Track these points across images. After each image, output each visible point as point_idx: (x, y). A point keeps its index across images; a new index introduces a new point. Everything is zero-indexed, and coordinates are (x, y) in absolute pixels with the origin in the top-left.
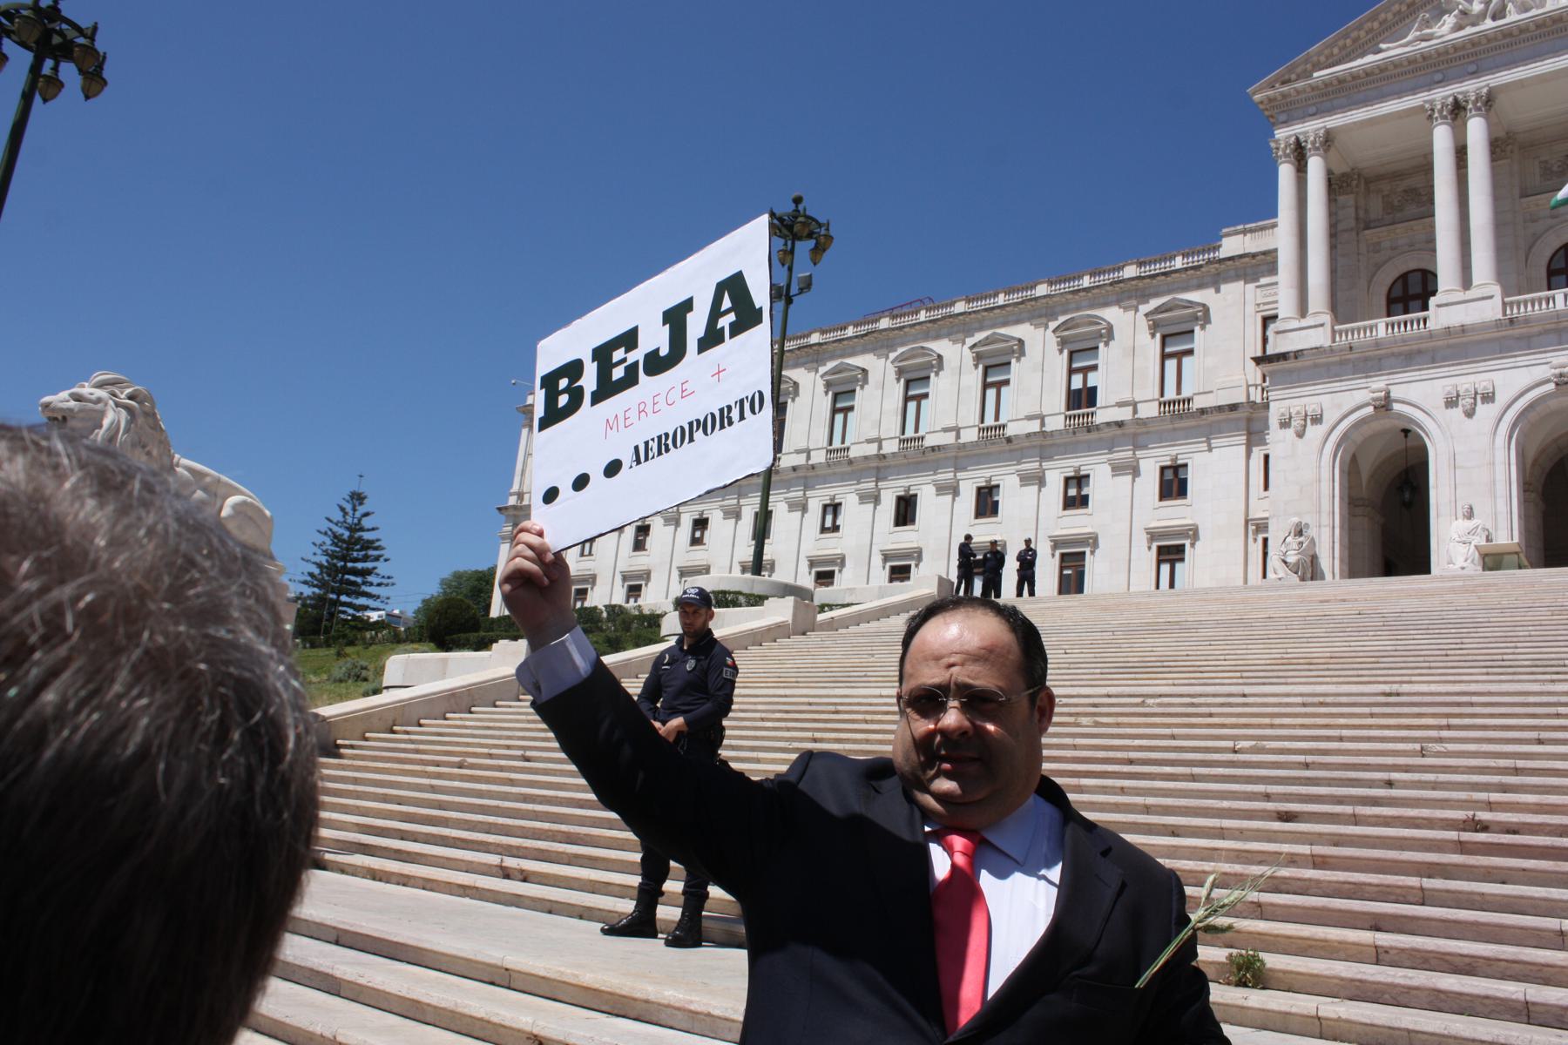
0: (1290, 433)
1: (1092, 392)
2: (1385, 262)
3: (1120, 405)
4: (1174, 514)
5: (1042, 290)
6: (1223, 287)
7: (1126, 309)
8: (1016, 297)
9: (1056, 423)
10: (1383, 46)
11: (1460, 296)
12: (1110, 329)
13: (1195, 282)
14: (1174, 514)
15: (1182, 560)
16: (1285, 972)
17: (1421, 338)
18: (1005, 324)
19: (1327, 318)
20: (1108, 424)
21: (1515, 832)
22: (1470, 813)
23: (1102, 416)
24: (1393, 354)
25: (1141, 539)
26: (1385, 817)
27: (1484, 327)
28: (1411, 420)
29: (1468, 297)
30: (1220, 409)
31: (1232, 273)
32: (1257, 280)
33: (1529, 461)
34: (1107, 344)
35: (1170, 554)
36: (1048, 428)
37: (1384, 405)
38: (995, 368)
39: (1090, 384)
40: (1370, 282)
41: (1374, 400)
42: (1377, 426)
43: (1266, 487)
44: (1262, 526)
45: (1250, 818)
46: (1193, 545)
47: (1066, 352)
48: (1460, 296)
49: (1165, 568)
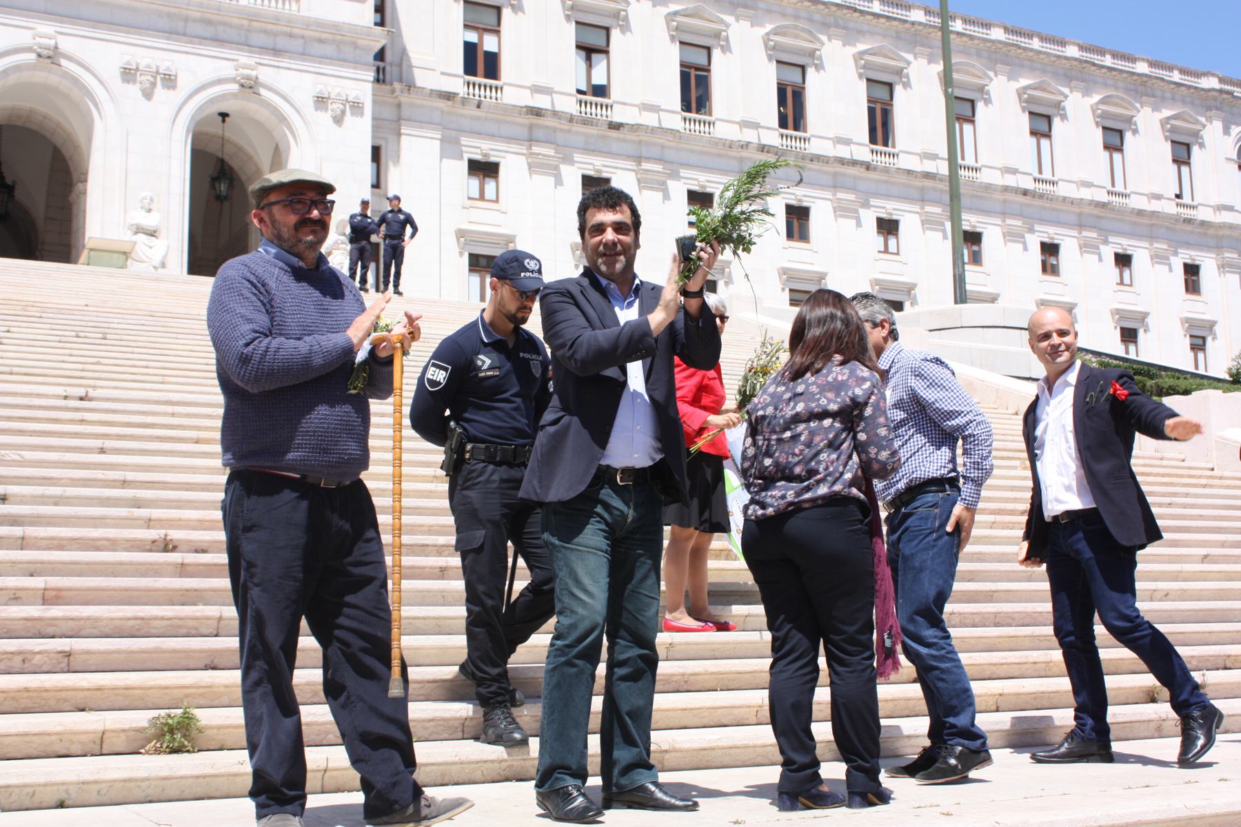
16: (219, 728)
21: (204, 551)
22: (162, 532)
26: (62, 539)
45: (61, 547)
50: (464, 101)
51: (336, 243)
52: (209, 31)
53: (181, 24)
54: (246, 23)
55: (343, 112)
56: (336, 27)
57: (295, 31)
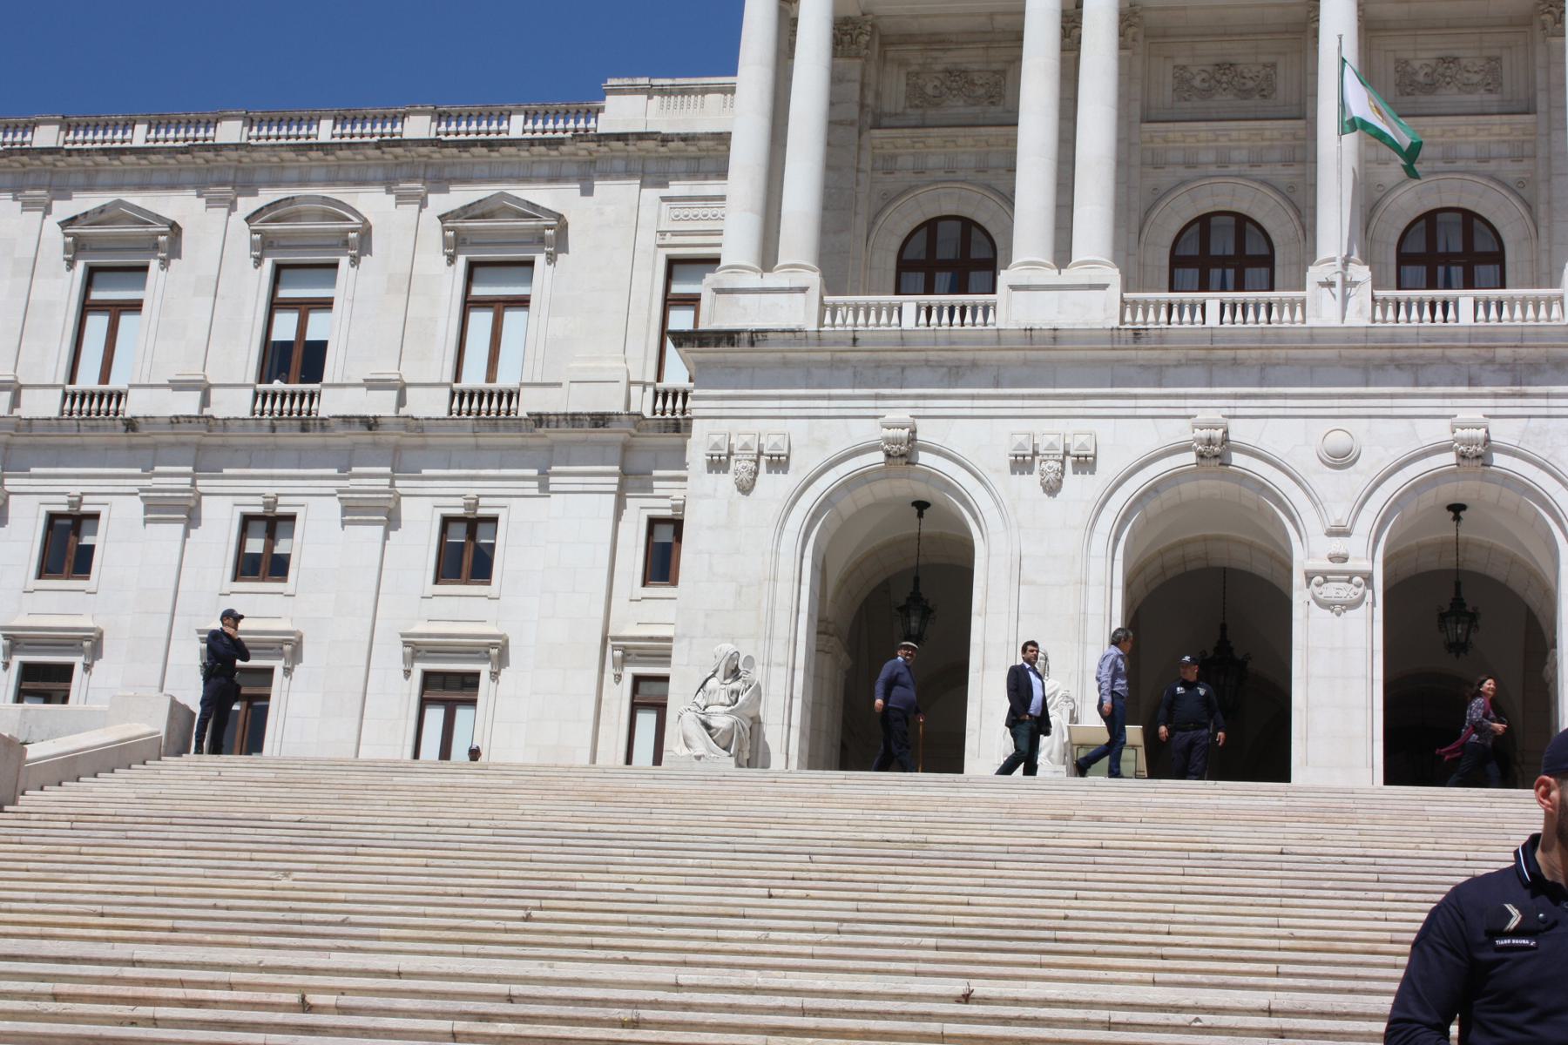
0: (726, 481)
1: (317, 351)
2: (904, 192)
3: (372, 385)
4: (461, 612)
5: (230, 131)
6: (600, 187)
7: (402, 199)
8: (172, 137)
9: (234, 404)
11: (1051, 276)
12: (366, 233)
13: (545, 170)
14: (461, 612)
15: (472, 703)
17: (980, 341)
18: (142, 187)
19: (813, 279)
20: (347, 420)
23: (331, 403)
24: (927, 363)
25: (391, 655)
27: (1088, 338)
28: (949, 486)
29: (1064, 274)
30: (574, 419)
31: (619, 165)
32: (665, 185)
34: (355, 261)
35: (449, 689)
36: (25, 411)
37: (903, 454)
38: (112, 271)
39: (311, 336)
40: (872, 224)
41: (888, 441)
42: (882, 489)
46: (494, 676)
47: (268, 264)
49: (435, 716)
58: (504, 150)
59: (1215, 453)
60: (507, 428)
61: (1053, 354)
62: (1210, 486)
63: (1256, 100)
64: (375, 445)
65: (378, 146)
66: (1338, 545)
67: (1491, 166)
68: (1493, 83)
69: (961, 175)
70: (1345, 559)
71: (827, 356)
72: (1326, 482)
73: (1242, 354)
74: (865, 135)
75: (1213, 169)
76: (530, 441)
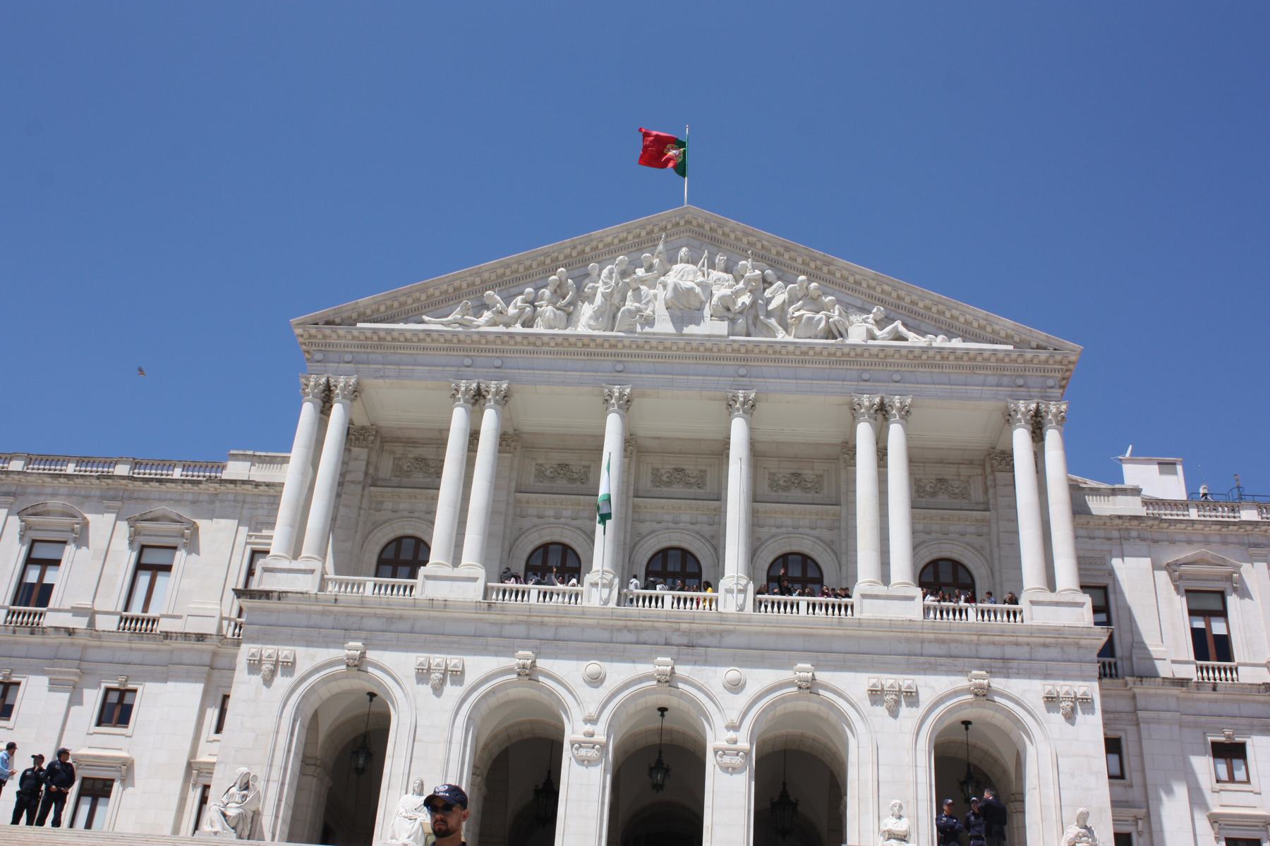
2: (385, 522)
10: (426, 318)
11: (448, 571)
13: (190, 497)
17: (404, 605)
24: (375, 615)
27: (464, 606)
28: (380, 685)
30: (186, 636)
33: (481, 744)
37: (358, 665)
39: (46, 581)
42: (346, 684)
43: (219, 729)
44: (208, 769)
48: (448, 571)
50: (1199, 685)
51: (1077, 836)
52: (943, 650)
53: (919, 646)
54: (975, 638)
55: (1073, 709)
56: (1058, 632)
57: (1020, 639)
58: (169, 485)
59: (529, 673)
60: (148, 639)
61: (444, 614)
62: (524, 691)
63: (578, 484)
64: (72, 644)
65: (98, 478)
66: (589, 728)
67: (697, 527)
68: (700, 485)
69: (416, 514)
70: (592, 735)
71: (320, 608)
72: (585, 692)
73: (546, 619)
74: (366, 491)
75: (552, 520)
76: (163, 647)
